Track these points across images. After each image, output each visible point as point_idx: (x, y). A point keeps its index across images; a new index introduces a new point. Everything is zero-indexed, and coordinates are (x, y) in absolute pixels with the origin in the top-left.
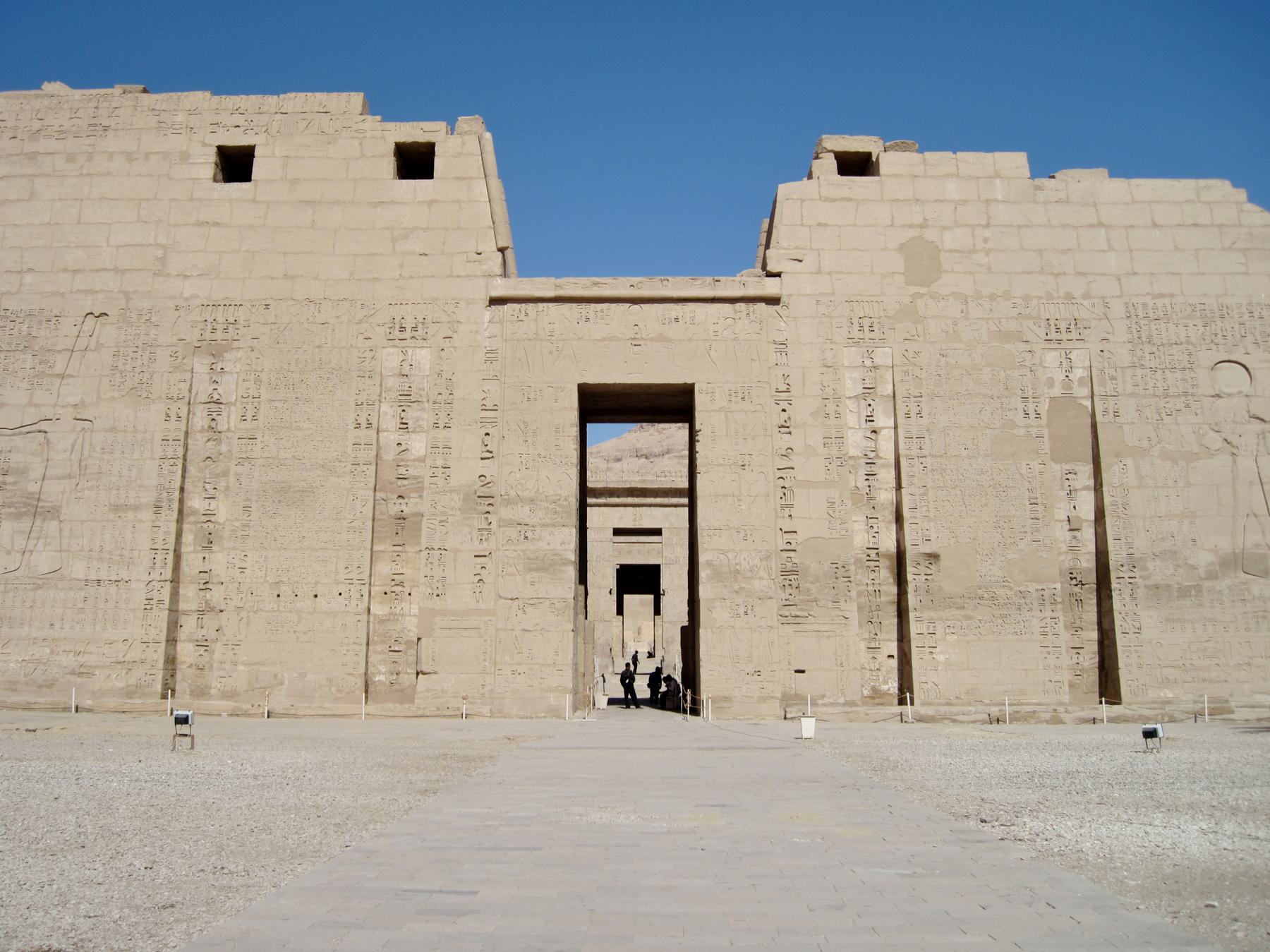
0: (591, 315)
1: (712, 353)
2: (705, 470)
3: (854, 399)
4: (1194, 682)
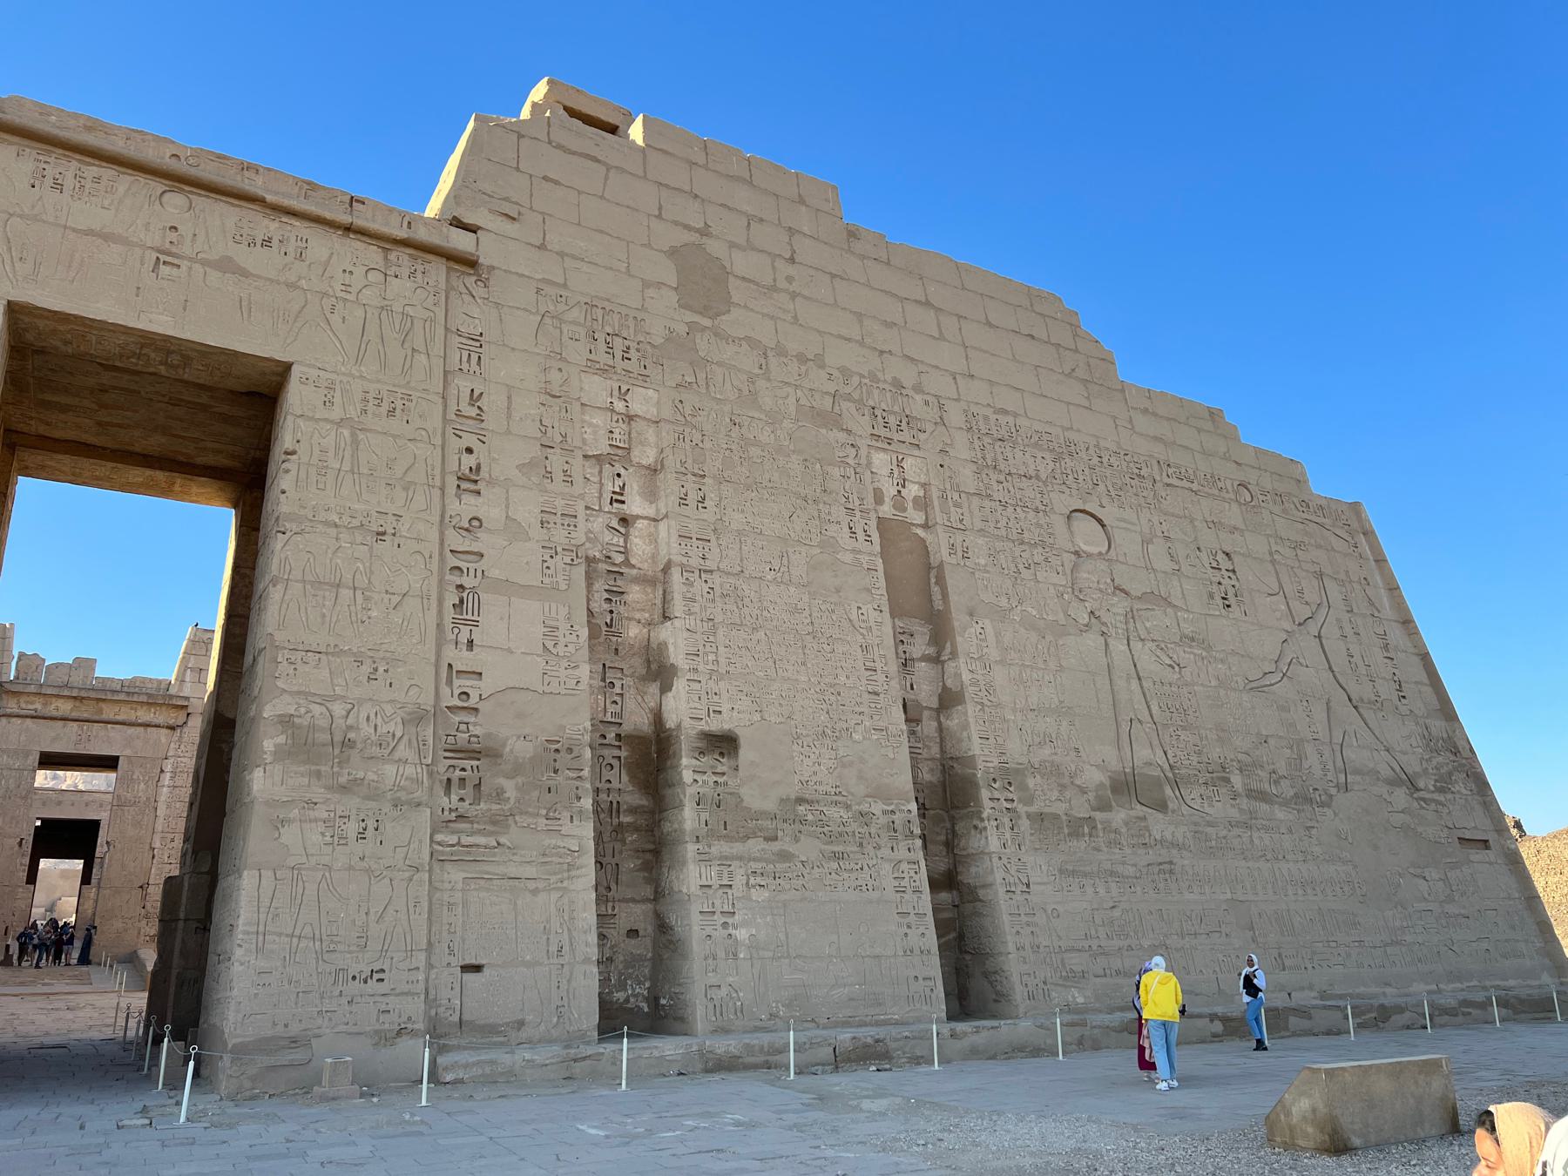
0: (69, 182)
1: (335, 319)
2: (298, 530)
3: (593, 461)
4: (1105, 976)
